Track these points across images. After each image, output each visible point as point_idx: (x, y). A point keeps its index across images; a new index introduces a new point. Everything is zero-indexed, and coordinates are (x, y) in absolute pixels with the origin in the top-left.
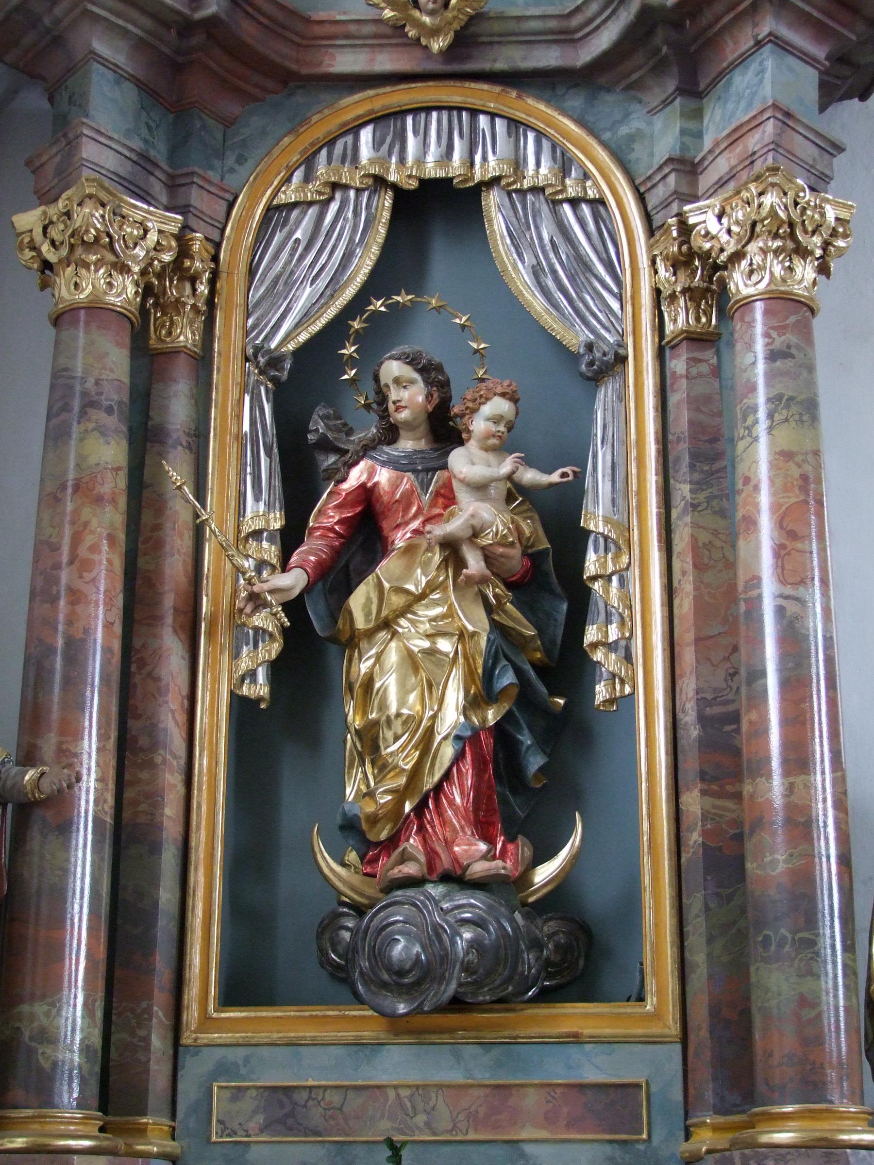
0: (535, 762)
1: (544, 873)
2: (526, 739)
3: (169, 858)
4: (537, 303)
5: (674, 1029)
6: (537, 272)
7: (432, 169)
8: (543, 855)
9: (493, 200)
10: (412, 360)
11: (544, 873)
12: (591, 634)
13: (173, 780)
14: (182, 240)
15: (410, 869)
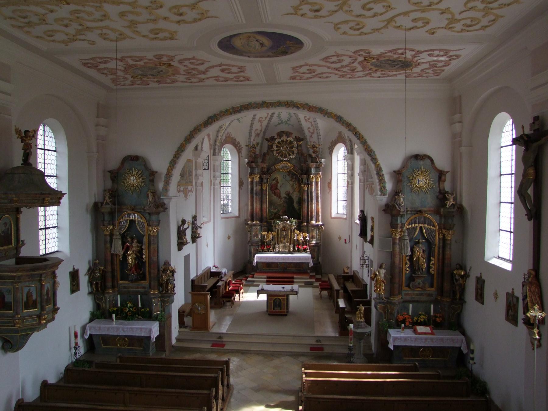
0: (140, 264)
1: (141, 272)
2: (139, 262)
3: (116, 272)
4: (139, 230)
5: (148, 283)
6: (139, 227)
7: (132, 219)
8: (141, 271)
9: (136, 221)
10: (129, 237)
11: (141, 272)
12: (143, 256)
13: (116, 266)
14: (113, 227)
15: (131, 273)
